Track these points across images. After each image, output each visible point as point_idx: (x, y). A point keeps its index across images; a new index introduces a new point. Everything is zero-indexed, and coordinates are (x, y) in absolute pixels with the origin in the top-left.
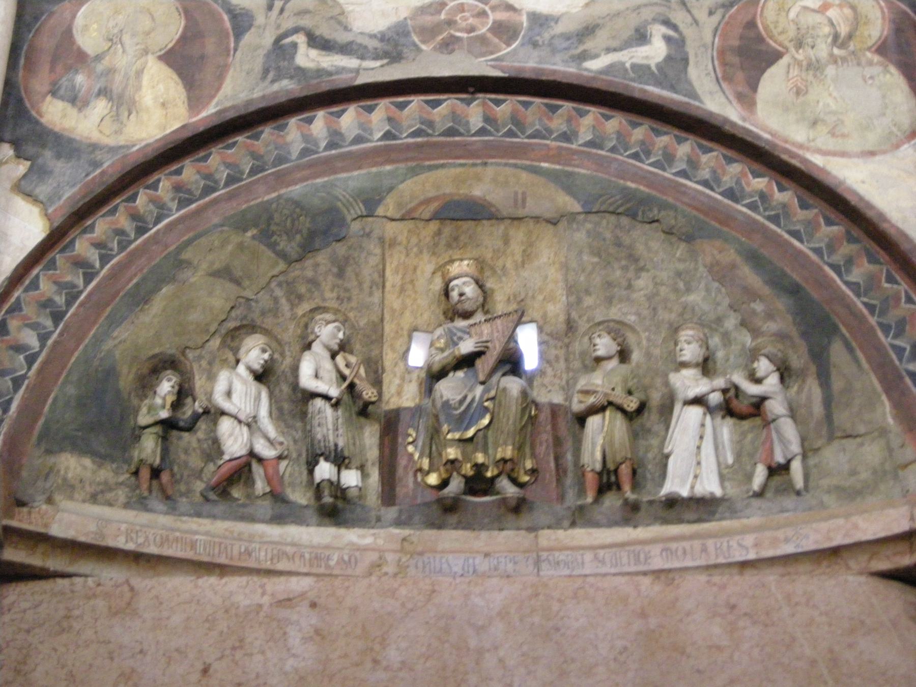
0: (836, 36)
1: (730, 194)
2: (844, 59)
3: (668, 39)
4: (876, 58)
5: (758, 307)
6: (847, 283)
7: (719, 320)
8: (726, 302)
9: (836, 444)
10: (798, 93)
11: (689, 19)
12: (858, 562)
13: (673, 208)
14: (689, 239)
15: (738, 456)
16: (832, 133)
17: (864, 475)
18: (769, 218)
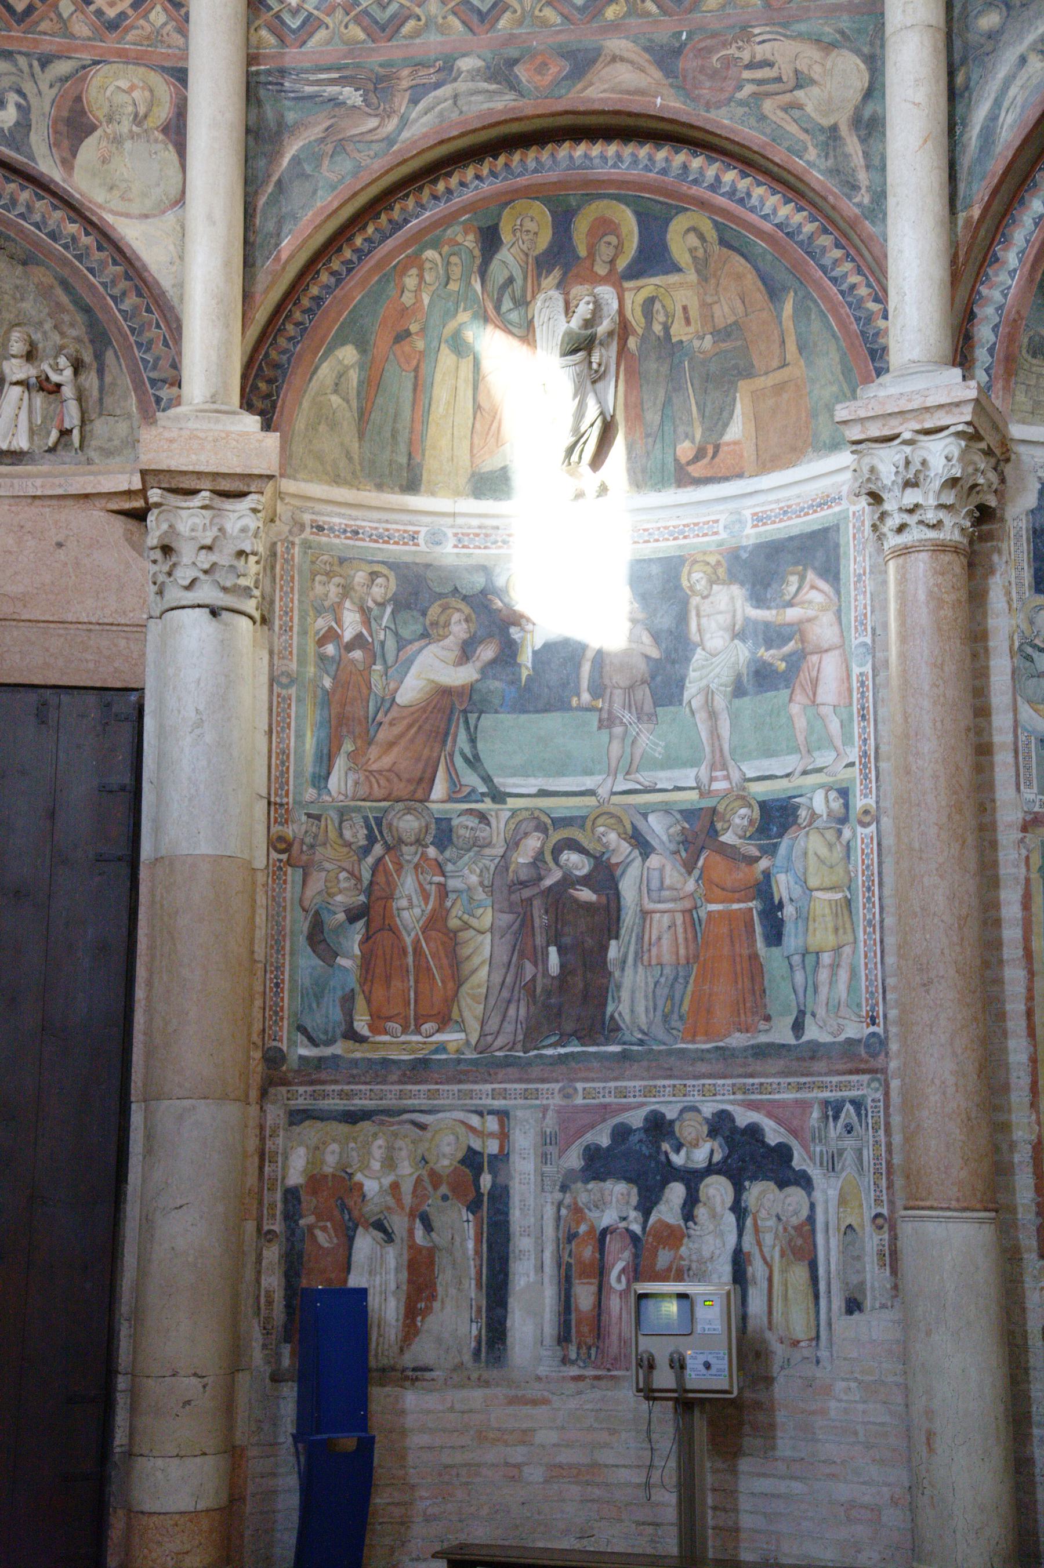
0: (136, 115)
1: (53, 236)
2: (138, 135)
3: (19, 106)
4: (161, 137)
5: (66, 318)
6: (119, 310)
7: (41, 323)
8: (47, 310)
9: (103, 418)
10: (104, 161)
11: (36, 90)
12: (101, 503)
13: (13, 240)
14: (24, 263)
15: (44, 418)
16: (122, 198)
17: (117, 442)
18: (75, 256)
